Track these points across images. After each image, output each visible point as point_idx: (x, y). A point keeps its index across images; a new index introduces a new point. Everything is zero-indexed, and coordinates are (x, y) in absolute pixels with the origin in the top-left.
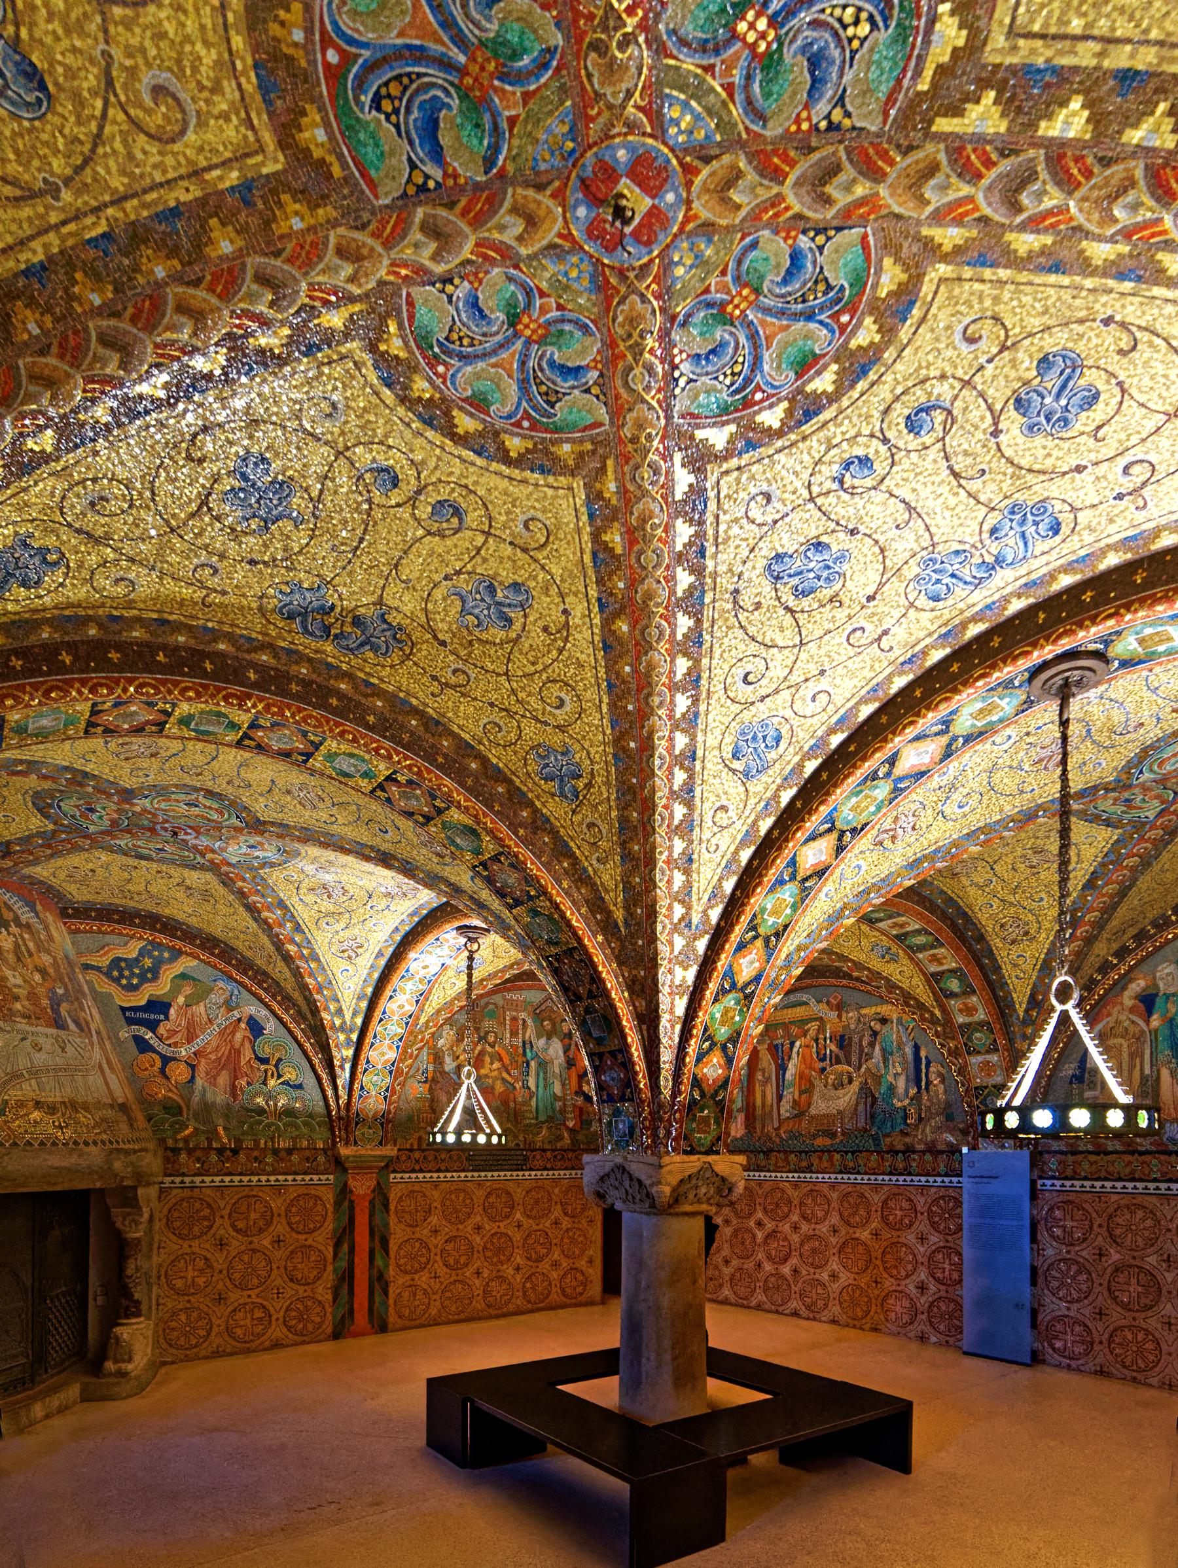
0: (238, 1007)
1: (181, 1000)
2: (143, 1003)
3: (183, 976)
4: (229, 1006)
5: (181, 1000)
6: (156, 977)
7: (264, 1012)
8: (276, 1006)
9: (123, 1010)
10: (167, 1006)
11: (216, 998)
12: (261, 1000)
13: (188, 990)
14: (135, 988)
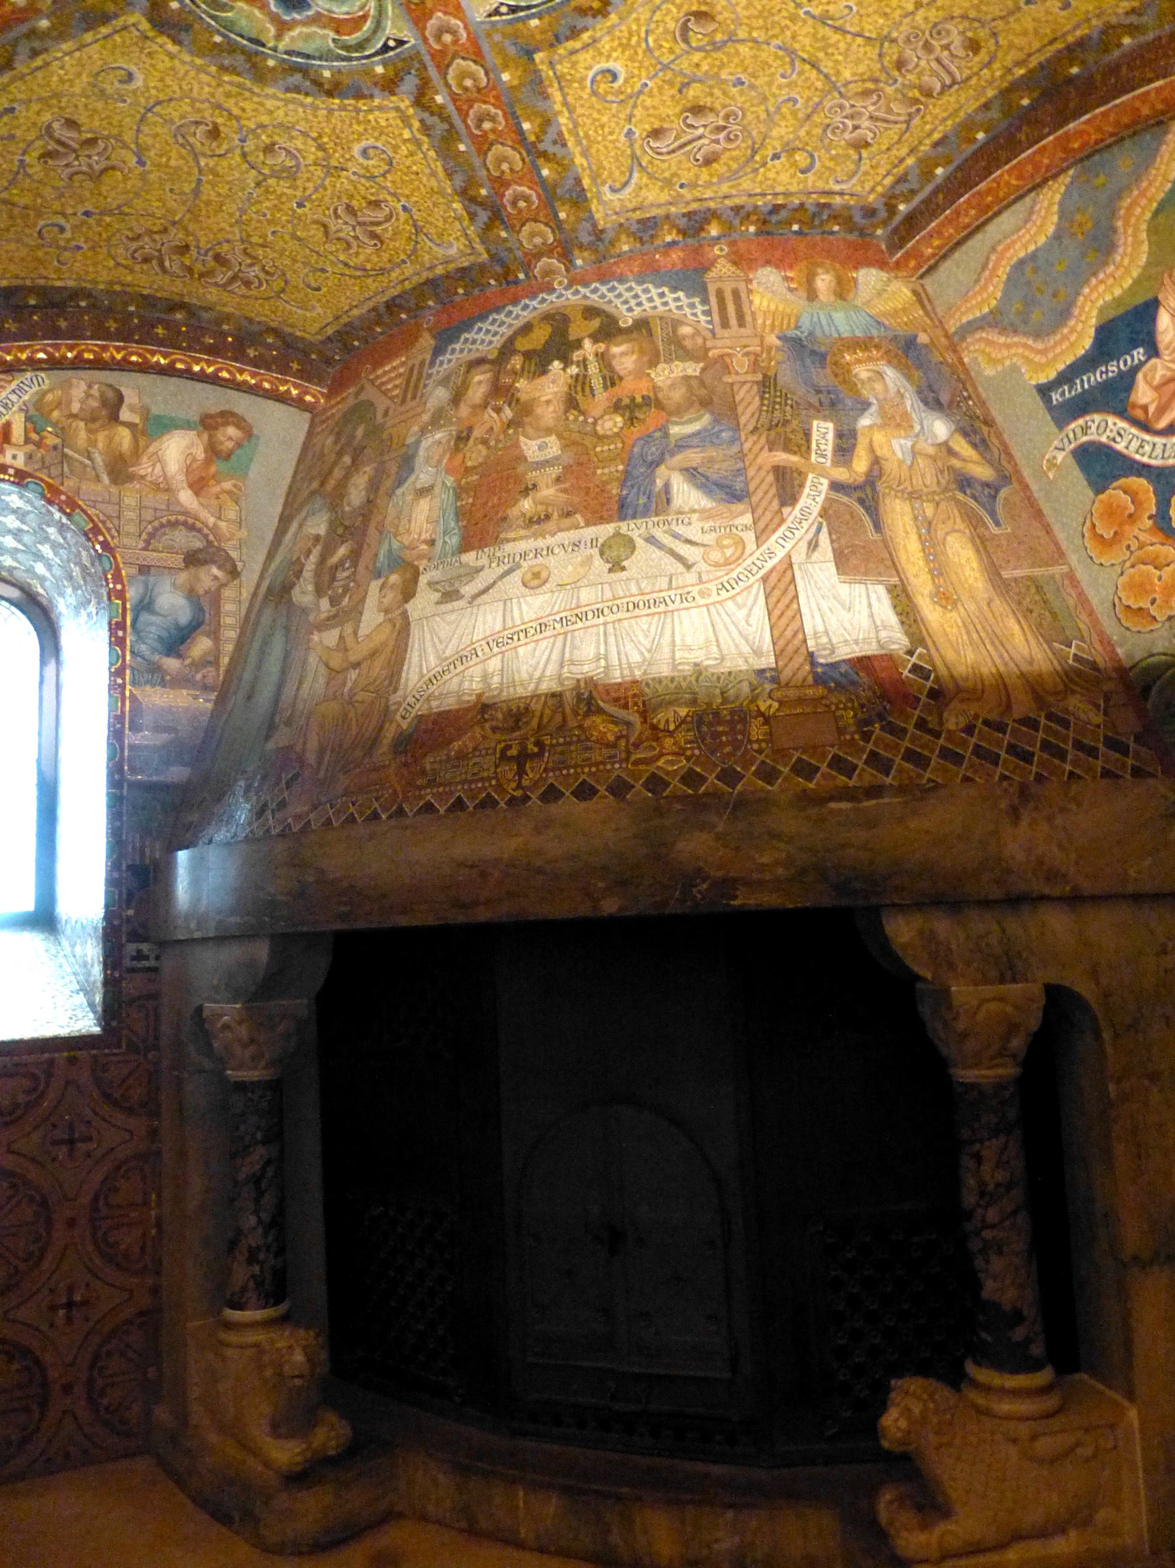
9: (1044, 391)
14: (1065, 314)
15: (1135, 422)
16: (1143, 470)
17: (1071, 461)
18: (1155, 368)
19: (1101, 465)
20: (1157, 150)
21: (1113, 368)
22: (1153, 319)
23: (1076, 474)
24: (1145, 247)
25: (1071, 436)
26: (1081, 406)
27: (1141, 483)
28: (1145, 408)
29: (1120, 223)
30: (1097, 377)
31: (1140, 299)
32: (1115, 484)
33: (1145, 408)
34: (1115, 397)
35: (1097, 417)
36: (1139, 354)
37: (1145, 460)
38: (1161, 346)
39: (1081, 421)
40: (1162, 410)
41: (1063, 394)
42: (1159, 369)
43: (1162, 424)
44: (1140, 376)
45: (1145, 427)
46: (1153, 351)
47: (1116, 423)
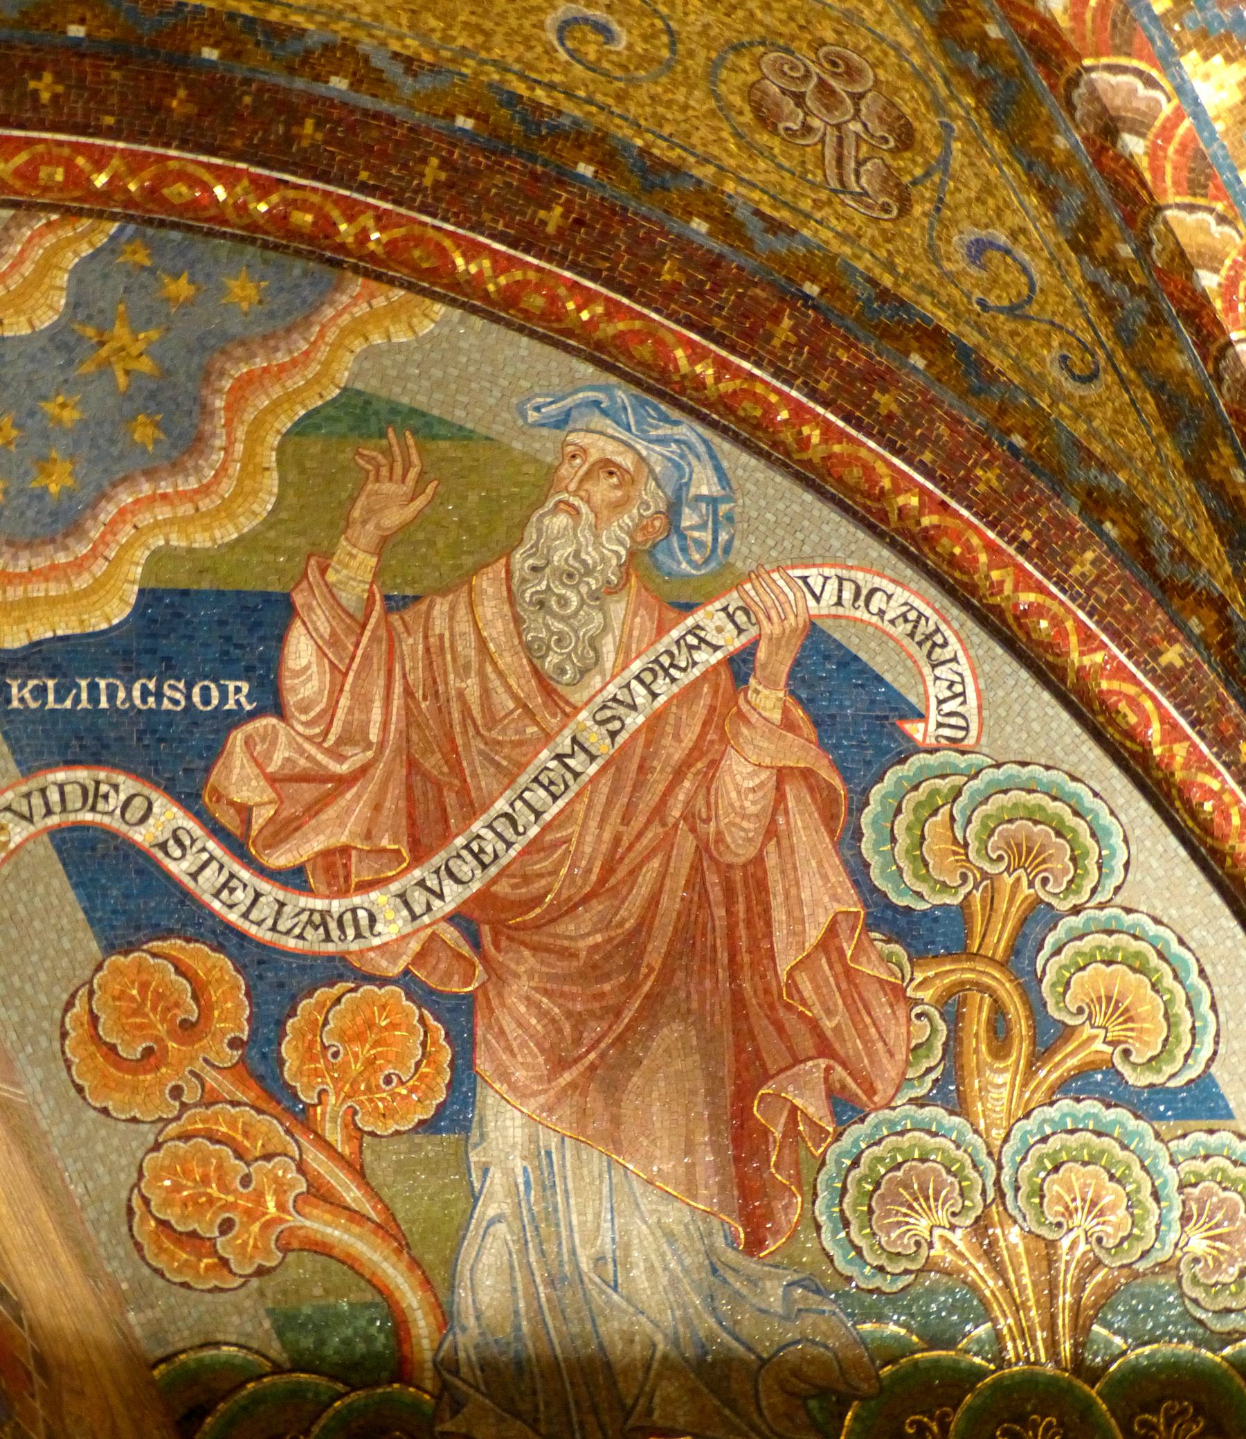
0: (723, 576)
1: (353, 570)
2: (114, 610)
3: (361, 414)
4: (663, 584)
5: (353, 570)
6: (186, 444)
7: (902, 595)
8: (972, 535)
10: (267, 616)
11: (580, 537)
12: (869, 512)
13: (392, 504)
14: (64, 522)
15: (217, 831)
16: (226, 938)
17: (45, 851)
18: (271, 739)
19: (123, 894)
20: (316, 309)
21: (174, 694)
22: (281, 638)
23: (56, 885)
24: (272, 481)
25: (54, 796)
26: (87, 741)
27: (217, 966)
28: (245, 812)
29: (219, 403)
30: (134, 695)
31: (255, 578)
32: (156, 945)
33: (245, 812)
34: (178, 757)
35: (128, 785)
36: (238, 693)
37: (233, 917)
38: (291, 699)
39: (82, 774)
40: (283, 830)
41: (40, 692)
42: (284, 744)
43: (281, 859)
44: (238, 737)
45: (238, 847)
46: (271, 701)
47: (168, 816)
